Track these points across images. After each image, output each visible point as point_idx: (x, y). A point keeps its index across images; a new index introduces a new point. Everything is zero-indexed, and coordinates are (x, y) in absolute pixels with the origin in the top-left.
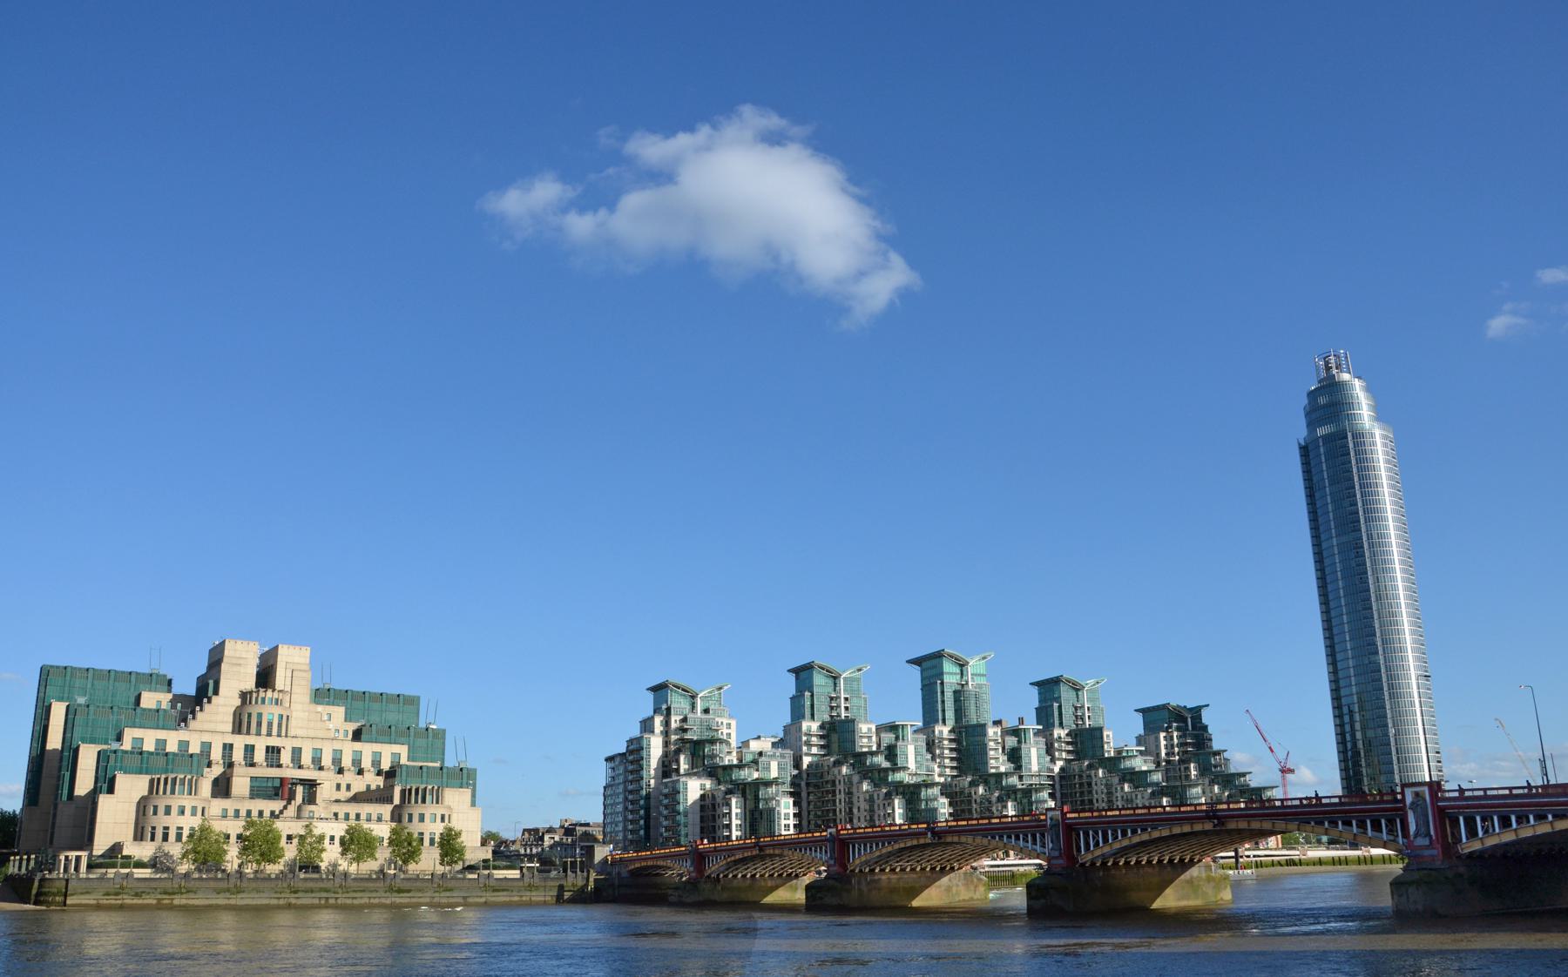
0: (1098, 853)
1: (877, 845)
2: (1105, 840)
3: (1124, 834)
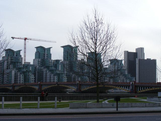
0: (84, 89)
1: (47, 86)
2: (87, 87)
3: (89, 86)
